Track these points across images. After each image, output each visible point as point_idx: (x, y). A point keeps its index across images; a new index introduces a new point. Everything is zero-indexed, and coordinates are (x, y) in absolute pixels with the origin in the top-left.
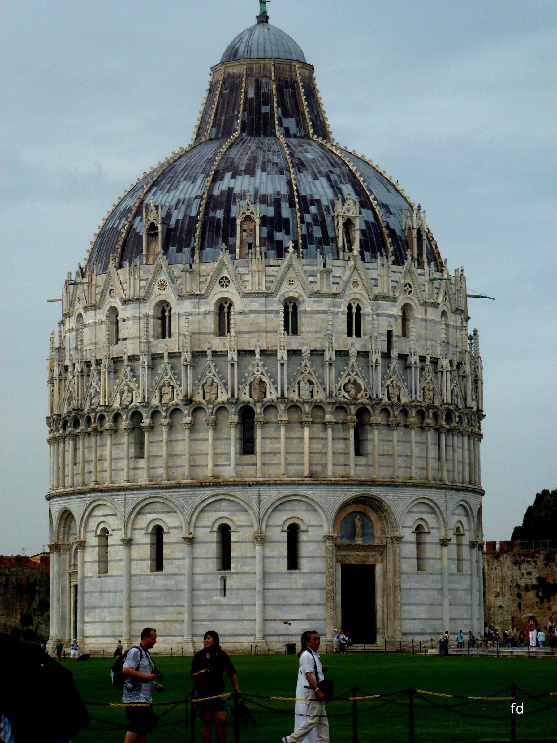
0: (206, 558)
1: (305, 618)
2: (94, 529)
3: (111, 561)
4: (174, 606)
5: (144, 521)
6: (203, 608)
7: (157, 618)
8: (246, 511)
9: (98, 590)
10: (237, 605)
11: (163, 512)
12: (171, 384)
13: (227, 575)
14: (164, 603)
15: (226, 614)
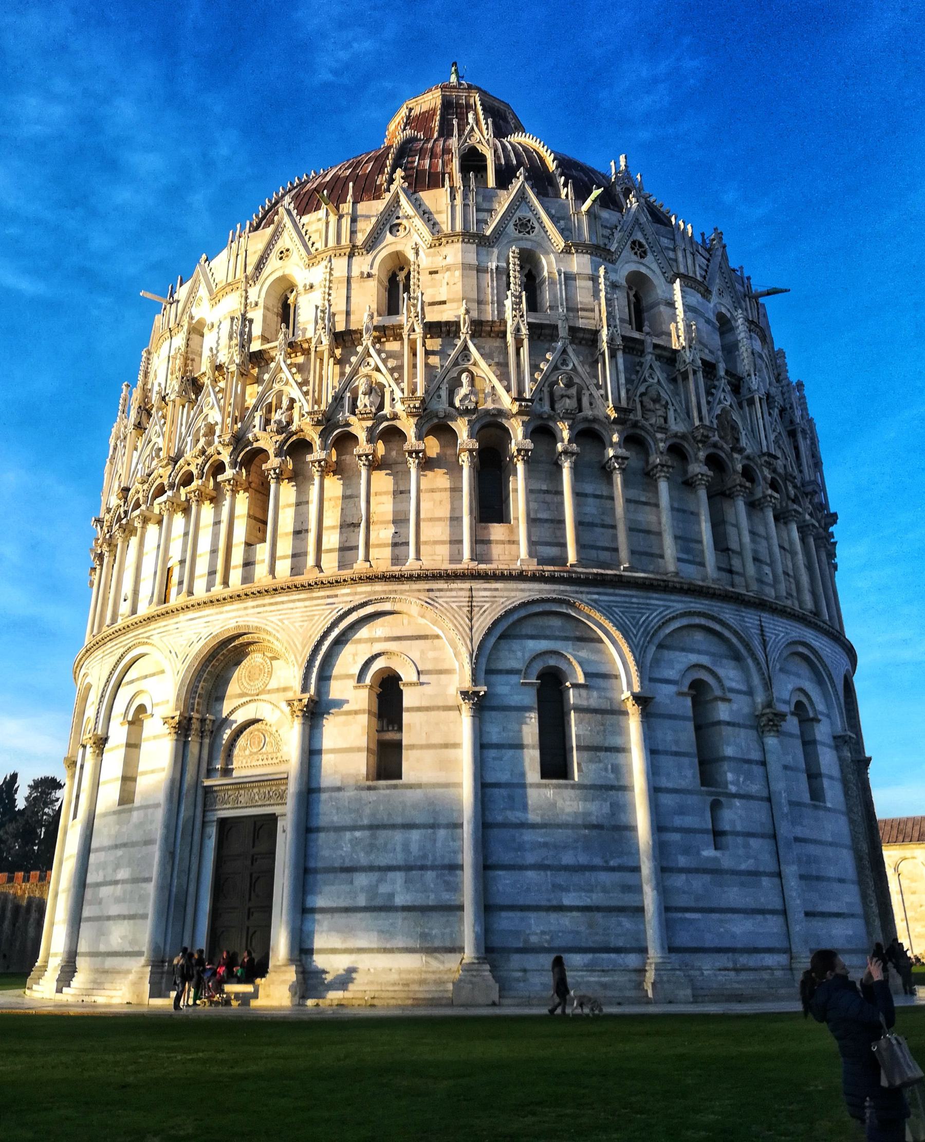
0: (676, 754)
1: (846, 911)
2: (356, 670)
3: (412, 747)
4: (613, 869)
5: (520, 653)
6: (683, 877)
7: (566, 902)
8: (737, 657)
9: (366, 822)
10: (750, 873)
11: (566, 639)
12: (576, 380)
13: (722, 799)
14: (583, 859)
15: (734, 895)
